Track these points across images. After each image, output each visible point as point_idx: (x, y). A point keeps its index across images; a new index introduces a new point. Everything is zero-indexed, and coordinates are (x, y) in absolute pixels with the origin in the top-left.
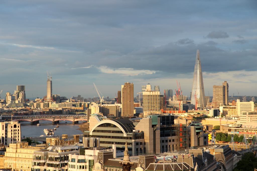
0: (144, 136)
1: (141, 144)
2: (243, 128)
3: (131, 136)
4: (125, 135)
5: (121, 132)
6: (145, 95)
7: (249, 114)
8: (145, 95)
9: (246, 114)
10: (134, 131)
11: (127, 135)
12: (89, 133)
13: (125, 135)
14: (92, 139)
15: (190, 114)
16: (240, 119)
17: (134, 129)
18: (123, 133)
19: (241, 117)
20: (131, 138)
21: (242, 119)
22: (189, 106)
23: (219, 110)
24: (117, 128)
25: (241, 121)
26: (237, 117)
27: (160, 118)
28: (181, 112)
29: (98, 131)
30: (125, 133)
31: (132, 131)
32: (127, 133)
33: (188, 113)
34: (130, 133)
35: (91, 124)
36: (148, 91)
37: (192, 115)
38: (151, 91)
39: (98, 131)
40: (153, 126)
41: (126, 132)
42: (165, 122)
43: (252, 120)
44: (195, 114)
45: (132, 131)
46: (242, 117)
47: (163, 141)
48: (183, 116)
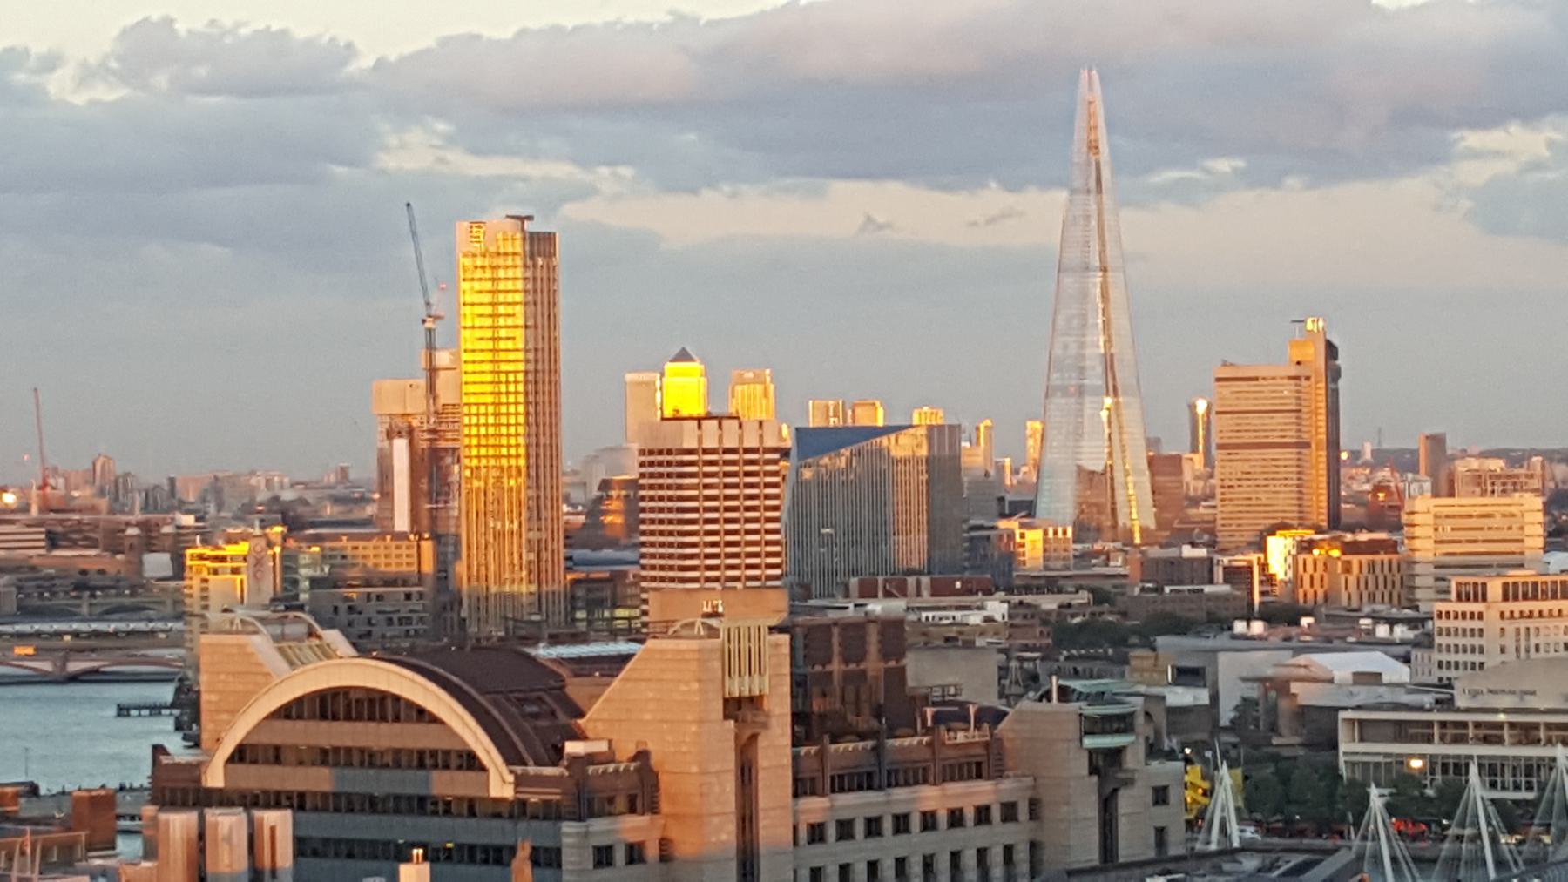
0: (655, 787)
1: (631, 860)
2: (1459, 710)
3: (554, 795)
4: (500, 784)
5: (471, 761)
6: (660, 452)
7: (1505, 598)
8: (660, 452)
9: (1484, 599)
10: (572, 747)
11: (520, 781)
12: (195, 770)
13: (500, 784)
14: (228, 823)
15: (1029, 606)
16: (1438, 640)
17: (579, 736)
18: (483, 769)
19: (1443, 623)
20: (552, 813)
21: (1452, 641)
22: (1022, 536)
23: (1264, 567)
24: (433, 726)
25: (1445, 657)
26: (1411, 623)
27: (785, 638)
28: (958, 585)
29: (276, 755)
30: (504, 769)
31: (562, 749)
32: (519, 769)
33: (1016, 599)
34: (549, 771)
35: (214, 698)
36: (685, 413)
37: (1049, 613)
38: (709, 417)
39: (276, 755)
40: (736, 707)
41: (511, 757)
42: (831, 673)
43: (1533, 641)
44: (1069, 606)
45: (559, 750)
46: (1452, 624)
47: (817, 833)
48: (975, 618)
